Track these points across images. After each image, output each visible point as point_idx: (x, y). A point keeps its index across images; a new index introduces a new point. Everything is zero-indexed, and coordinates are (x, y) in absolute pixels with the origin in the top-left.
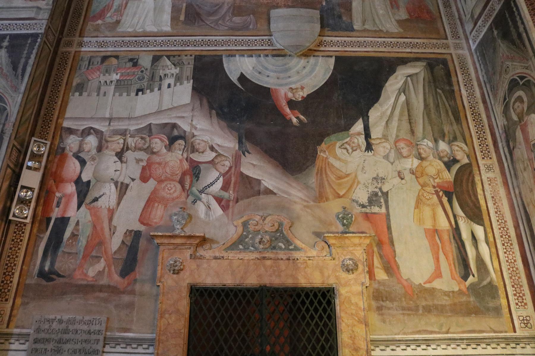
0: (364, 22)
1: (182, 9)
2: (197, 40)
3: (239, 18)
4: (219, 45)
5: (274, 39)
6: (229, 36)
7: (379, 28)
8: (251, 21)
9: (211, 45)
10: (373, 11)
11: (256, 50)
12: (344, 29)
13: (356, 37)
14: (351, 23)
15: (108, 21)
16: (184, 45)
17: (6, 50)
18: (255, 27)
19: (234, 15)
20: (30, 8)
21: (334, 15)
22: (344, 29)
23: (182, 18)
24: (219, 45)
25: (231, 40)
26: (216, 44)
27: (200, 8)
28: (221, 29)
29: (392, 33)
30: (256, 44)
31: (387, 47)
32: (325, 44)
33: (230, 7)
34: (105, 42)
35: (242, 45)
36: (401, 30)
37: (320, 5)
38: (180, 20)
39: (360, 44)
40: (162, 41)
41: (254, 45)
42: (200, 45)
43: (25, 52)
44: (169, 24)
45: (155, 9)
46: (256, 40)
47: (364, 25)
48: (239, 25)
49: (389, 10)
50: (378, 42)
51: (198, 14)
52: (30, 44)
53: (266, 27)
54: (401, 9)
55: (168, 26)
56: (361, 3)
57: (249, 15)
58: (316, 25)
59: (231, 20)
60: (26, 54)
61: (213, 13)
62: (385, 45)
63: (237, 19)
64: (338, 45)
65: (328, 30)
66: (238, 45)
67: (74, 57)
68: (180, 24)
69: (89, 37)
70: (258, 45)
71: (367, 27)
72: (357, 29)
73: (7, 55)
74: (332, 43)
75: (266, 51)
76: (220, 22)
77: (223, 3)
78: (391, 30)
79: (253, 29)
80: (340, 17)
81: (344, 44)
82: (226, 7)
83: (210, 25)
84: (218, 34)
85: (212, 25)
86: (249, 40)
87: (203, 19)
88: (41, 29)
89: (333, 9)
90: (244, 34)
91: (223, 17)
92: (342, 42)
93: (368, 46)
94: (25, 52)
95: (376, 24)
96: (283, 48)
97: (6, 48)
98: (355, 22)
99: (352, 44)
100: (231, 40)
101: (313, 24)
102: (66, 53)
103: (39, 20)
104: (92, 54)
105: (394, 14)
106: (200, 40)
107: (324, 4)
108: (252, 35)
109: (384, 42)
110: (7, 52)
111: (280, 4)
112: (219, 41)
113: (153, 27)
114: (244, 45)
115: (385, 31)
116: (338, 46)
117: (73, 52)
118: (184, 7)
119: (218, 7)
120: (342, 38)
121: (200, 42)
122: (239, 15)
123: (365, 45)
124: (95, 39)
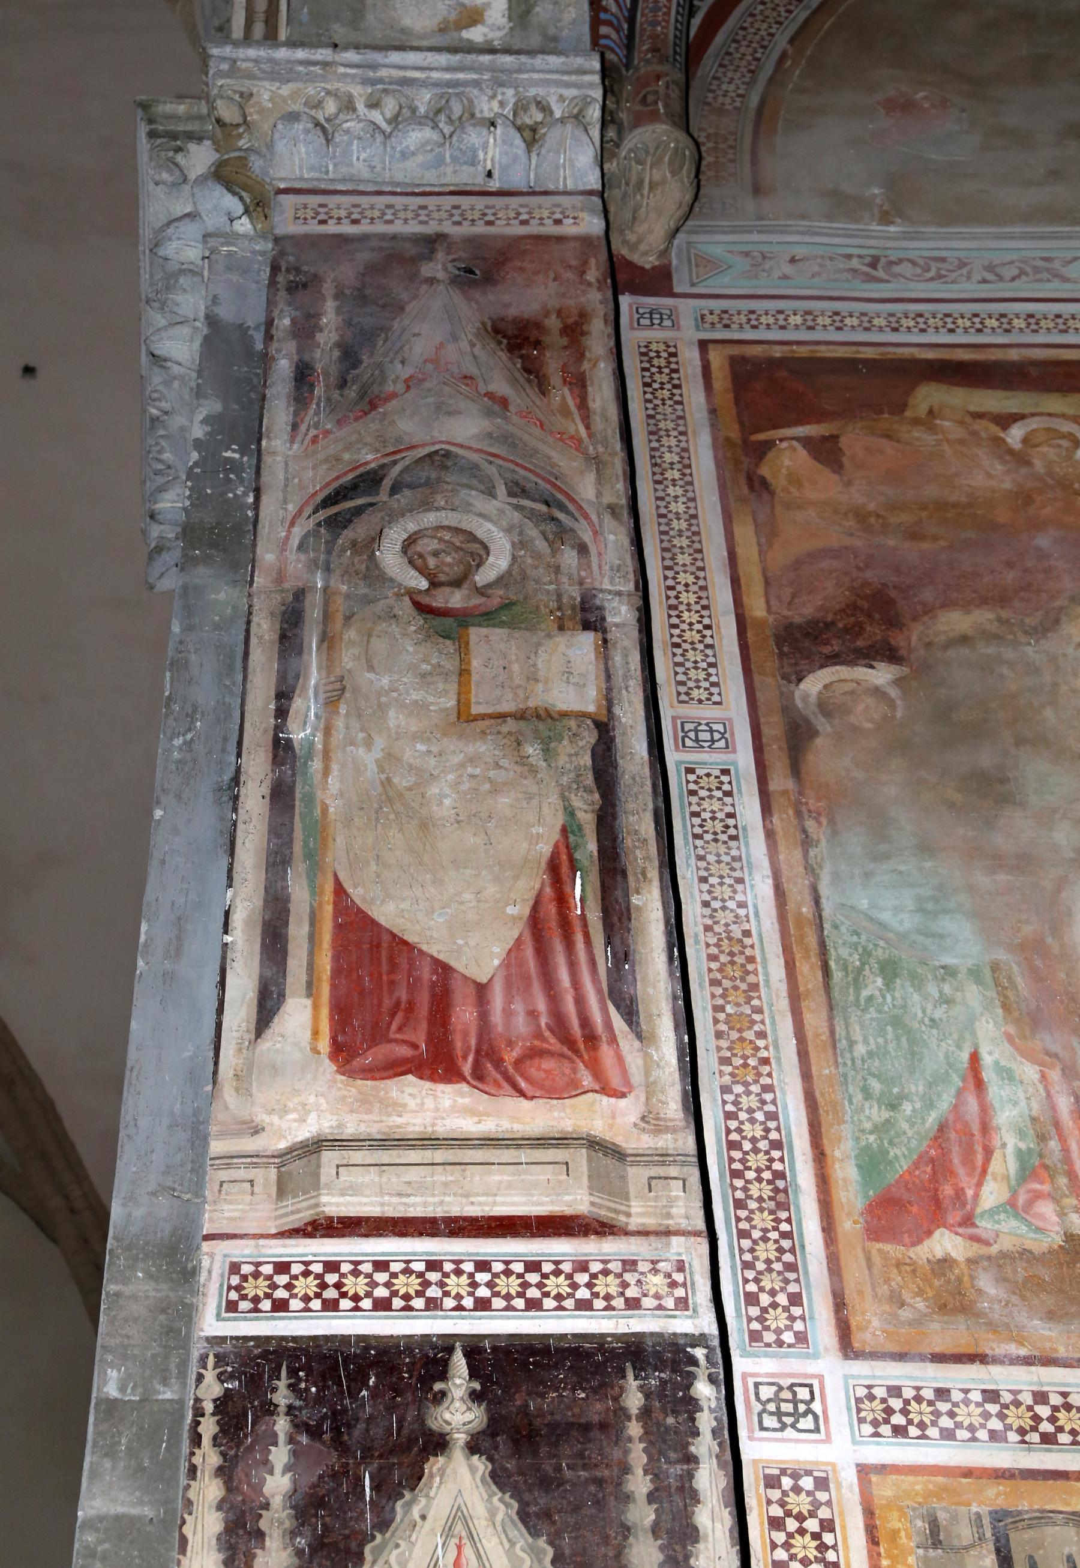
15: (1006, 1244)
17: (480, 1464)
20: (541, 1142)
34: (1056, 1400)
43: (639, 1484)
52: (646, 1413)
60: (651, 1498)
67: (869, 1513)
69: (922, 1358)
73: (504, 1507)
88: (683, 1304)
94: (639, 1484)
97: (473, 1448)
102: (796, 1476)
103: (643, 1233)
104: (995, 1495)
110: (498, 1478)
117: (849, 1477)
124: (956, 1376)
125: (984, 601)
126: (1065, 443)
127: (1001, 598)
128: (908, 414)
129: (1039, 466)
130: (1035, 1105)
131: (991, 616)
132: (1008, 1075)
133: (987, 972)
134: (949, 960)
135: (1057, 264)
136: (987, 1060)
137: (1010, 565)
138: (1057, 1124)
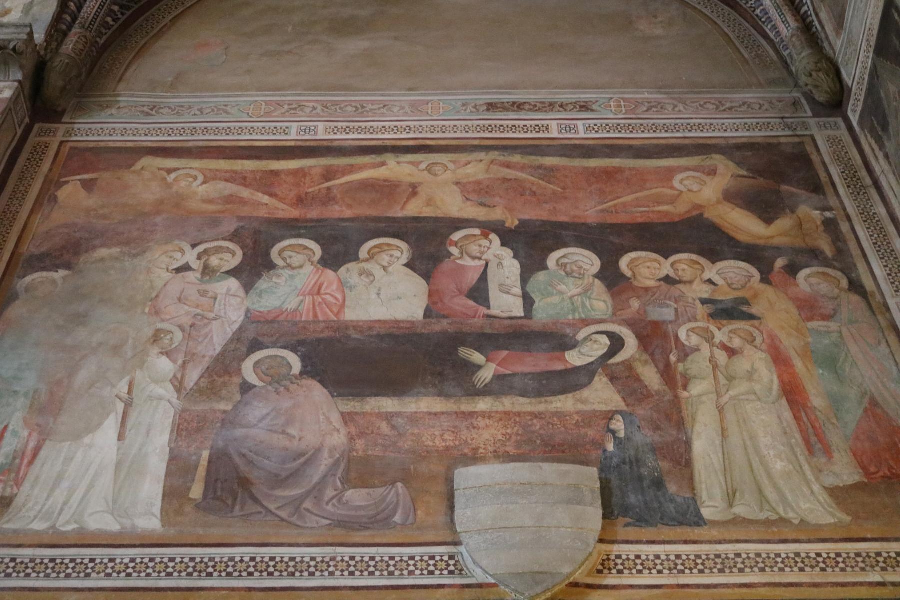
0: (731, 498)
1: (196, 467)
2: (238, 559)
3: (364, 491)
4: (302, 572)
5: (466, 555)
6: (332, 545)
7: (777, 513)
8: (398, 501)
9: (276, 574)
10: (756, 464)
11: (413, 587)
12: (673, 519)
13: (710, 542)
14: (694, 499)
16: (196, 574)
18: (411, 520)
19: (348, 482)
21: (641, 479)
22: (673, 519)
23: (197, 492)
24: (302, 572)
25: (339, 559)
26: (291, 570)
27: (250, 463)
28: (309, 525)
29: (819, 527)
30: (412, 568)
31: (808, 569)
32: (621, 567)
33: (336, 464)
35: (372, 574)
36: (847, 519)
37: (600, 452)
38: (190, 499)
39: (724, 564)
40: (133, 560)
41: (406, 573)
42: (244, 574)
44: (157, 510)
45: (119, 466)
46: (412, 558)
47: (731, 505)
48: (363, 513)
49: (802, 459)
50: (778, 555)
51: (245, 483)
53: (442, 519)
54: (836, 455)
55: (153, 515)
56: (718, 442)
57: (393, 483)
58: (590, 510)
59: (339, 497)
61: (288, 478)
62: (800, 565)
63: (357, 497)
64: (659, 567)
65: (627, 525)
66: (358, 573)
68: (188, 508)
70: (418, 572)
71: (740, 510)
72: (712, 518)
74: (639, 562)
75: (441, 591)
76: (308, 504)
77: (319, 450)
78: (812, 519)
79: (403, 525)
80: (659, 484)
81: (677, 565)
82: (325, 462)
83: (278, 513)
84: (301, 541)
85: (283, 514)
86: (392, 558)
87: (259, 496)
89: (637, 462)
90: (378, 540)
91: (317, 491)
92: (669, 560)
93: (747, 570)
95: (768, 502)
96: (493, 581)
98: (704, 499)
99: (698, 564)
100: (339, 559)
101: (579, 507)
105: (818, 471)
106: (247, 559)
107: (611, 447)
108: (400, 541)
109: (798, 555)
111: (481, 451)
112: (302, 562)
113: (109, 518)
114: (377, 573)
115: (796, 522)
116: (660, 572)
118: (204, 463)
119: (302, 460)
120: (668, 548)
121: (244, 565)
122: (363, 482)
123: (740, 566)
125: (119, 244)
126: (191, 180)
127: (127, 243)
128: (133, 169)
129: (175, 188)
130: (19, 446)
131: (119, 250)
132: (15, 433)
133: (31, 393)
134: (18, 389)
135: (228, 108)
136: (11, 428)
137: (139, 229)
138: (24, 454)
